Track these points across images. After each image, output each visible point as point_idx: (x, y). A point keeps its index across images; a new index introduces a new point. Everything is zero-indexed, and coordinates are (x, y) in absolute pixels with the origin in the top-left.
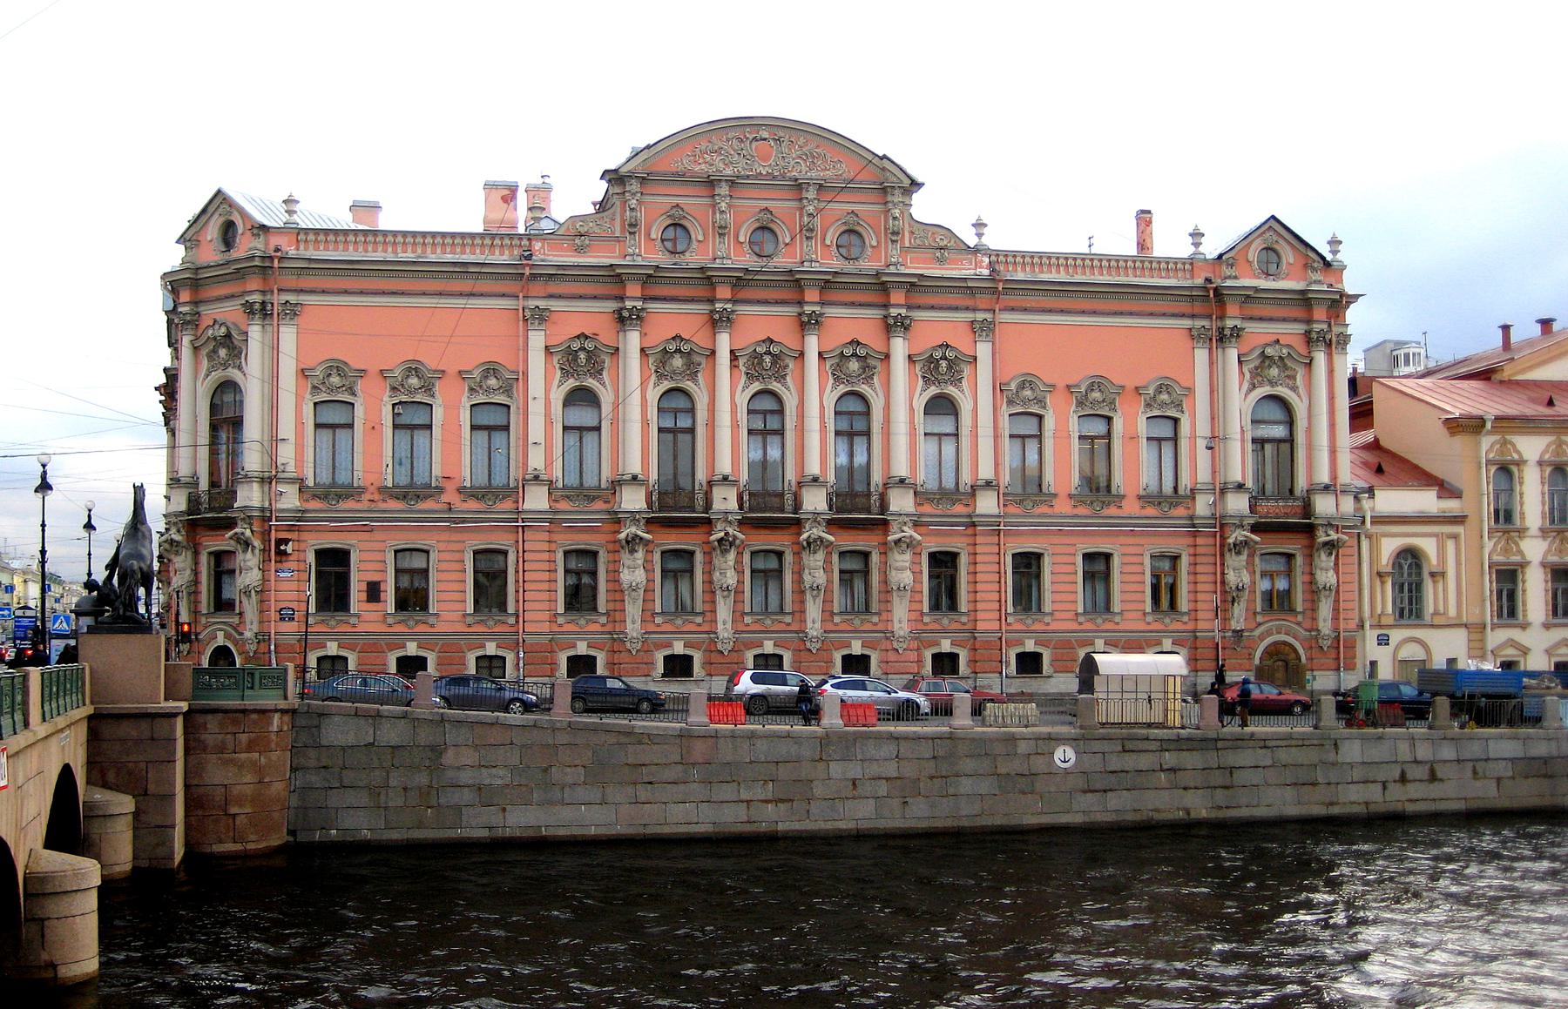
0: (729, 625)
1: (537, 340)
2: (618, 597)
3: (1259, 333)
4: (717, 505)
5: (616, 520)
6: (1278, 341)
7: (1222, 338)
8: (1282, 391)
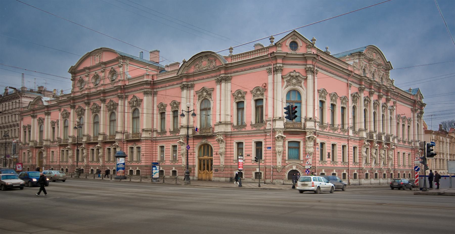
3: (288, 69)
6: (295, 71)
7: (276, 71)
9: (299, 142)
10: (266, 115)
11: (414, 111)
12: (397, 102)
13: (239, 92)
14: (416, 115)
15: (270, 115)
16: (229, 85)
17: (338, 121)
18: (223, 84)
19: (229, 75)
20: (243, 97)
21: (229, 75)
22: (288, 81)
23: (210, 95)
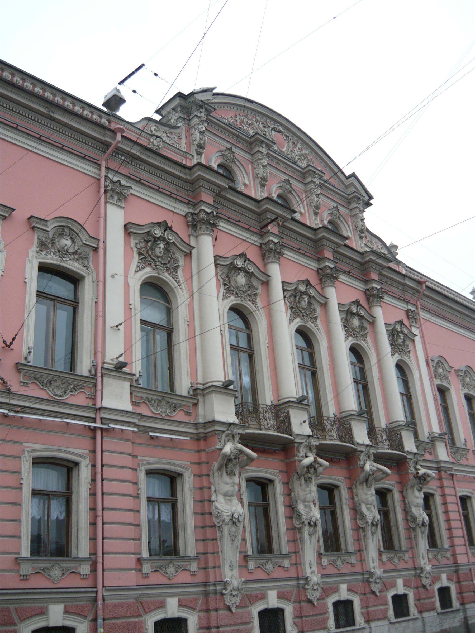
0: (315, 568)
1: (115, 218)
2: (209, 533)
4: (296, 429)
5: (206, 433)
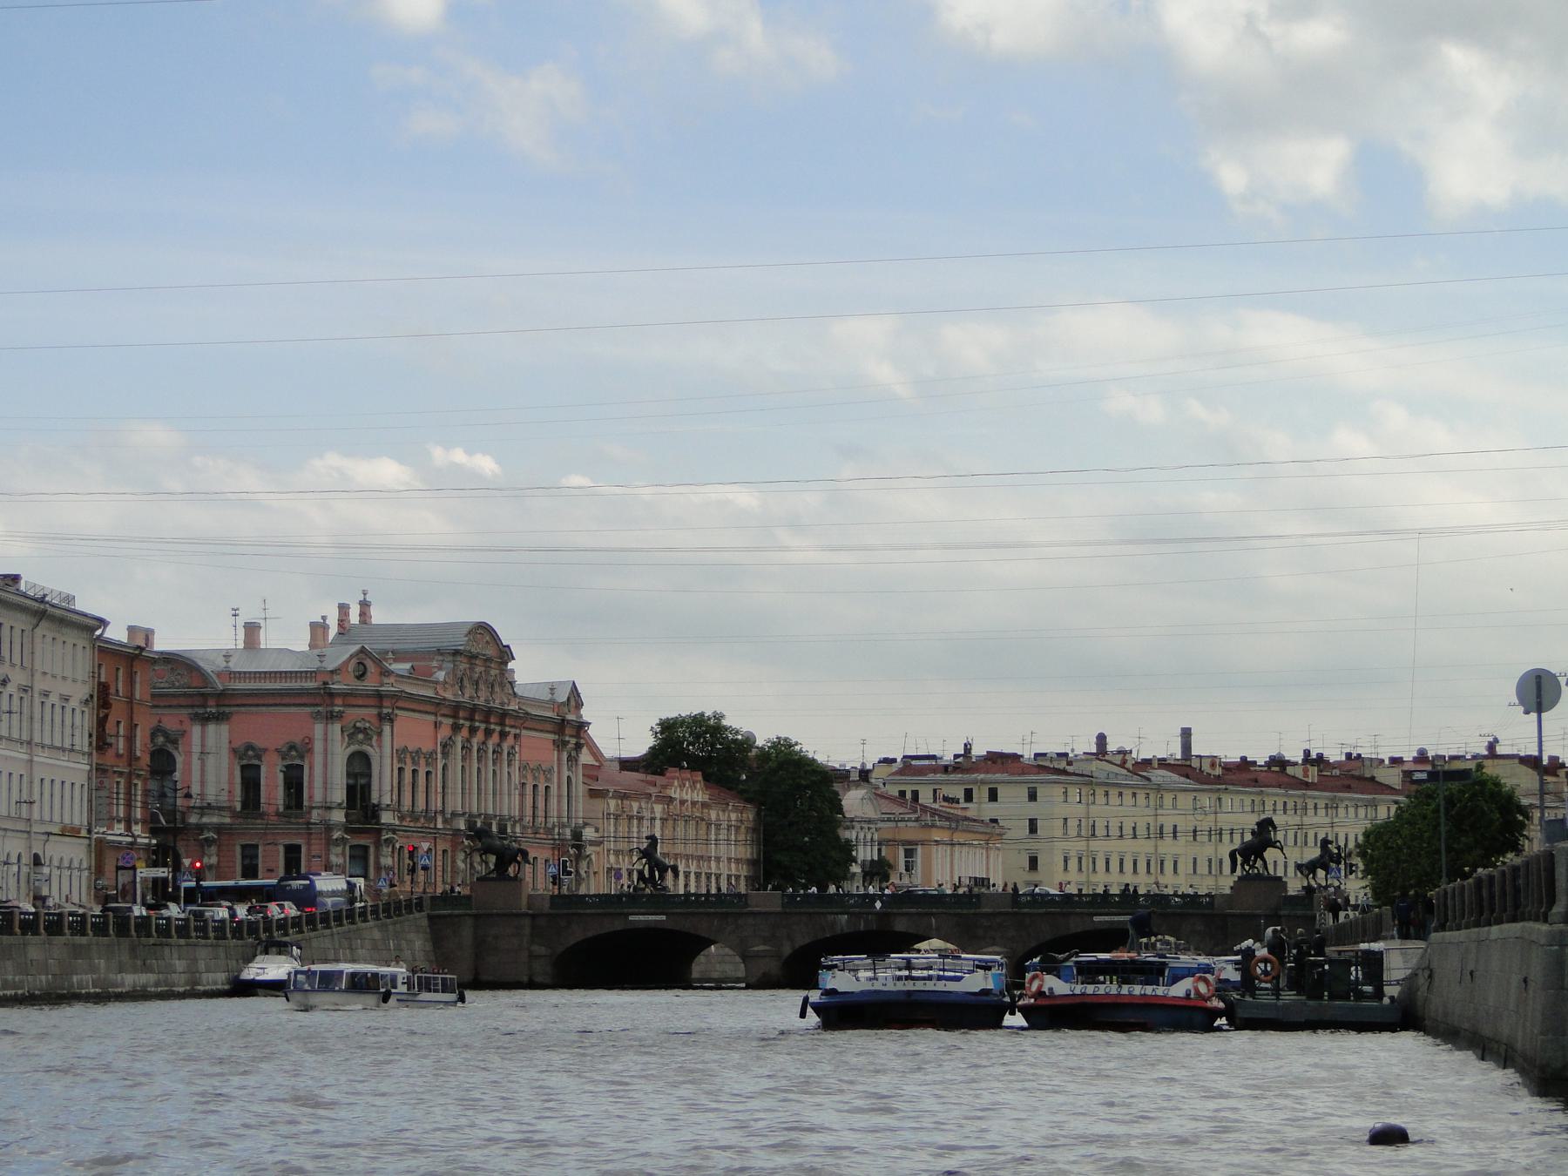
3: (355, 714)
7: (331, 717)
8: (366, 748)
9: (366, 848)
10: (311, 797)
11: (560, 745)
12: (524, 732)
13: (250, 747)
14: (565, 756)
15: (318, 797)
16: (224, 728)
17: (421, 805)
18: (211, 728)
19: (227, 710)
20: (259, 757)
21: (227, 710)
22: (351, 736)
23: (175, 742)
